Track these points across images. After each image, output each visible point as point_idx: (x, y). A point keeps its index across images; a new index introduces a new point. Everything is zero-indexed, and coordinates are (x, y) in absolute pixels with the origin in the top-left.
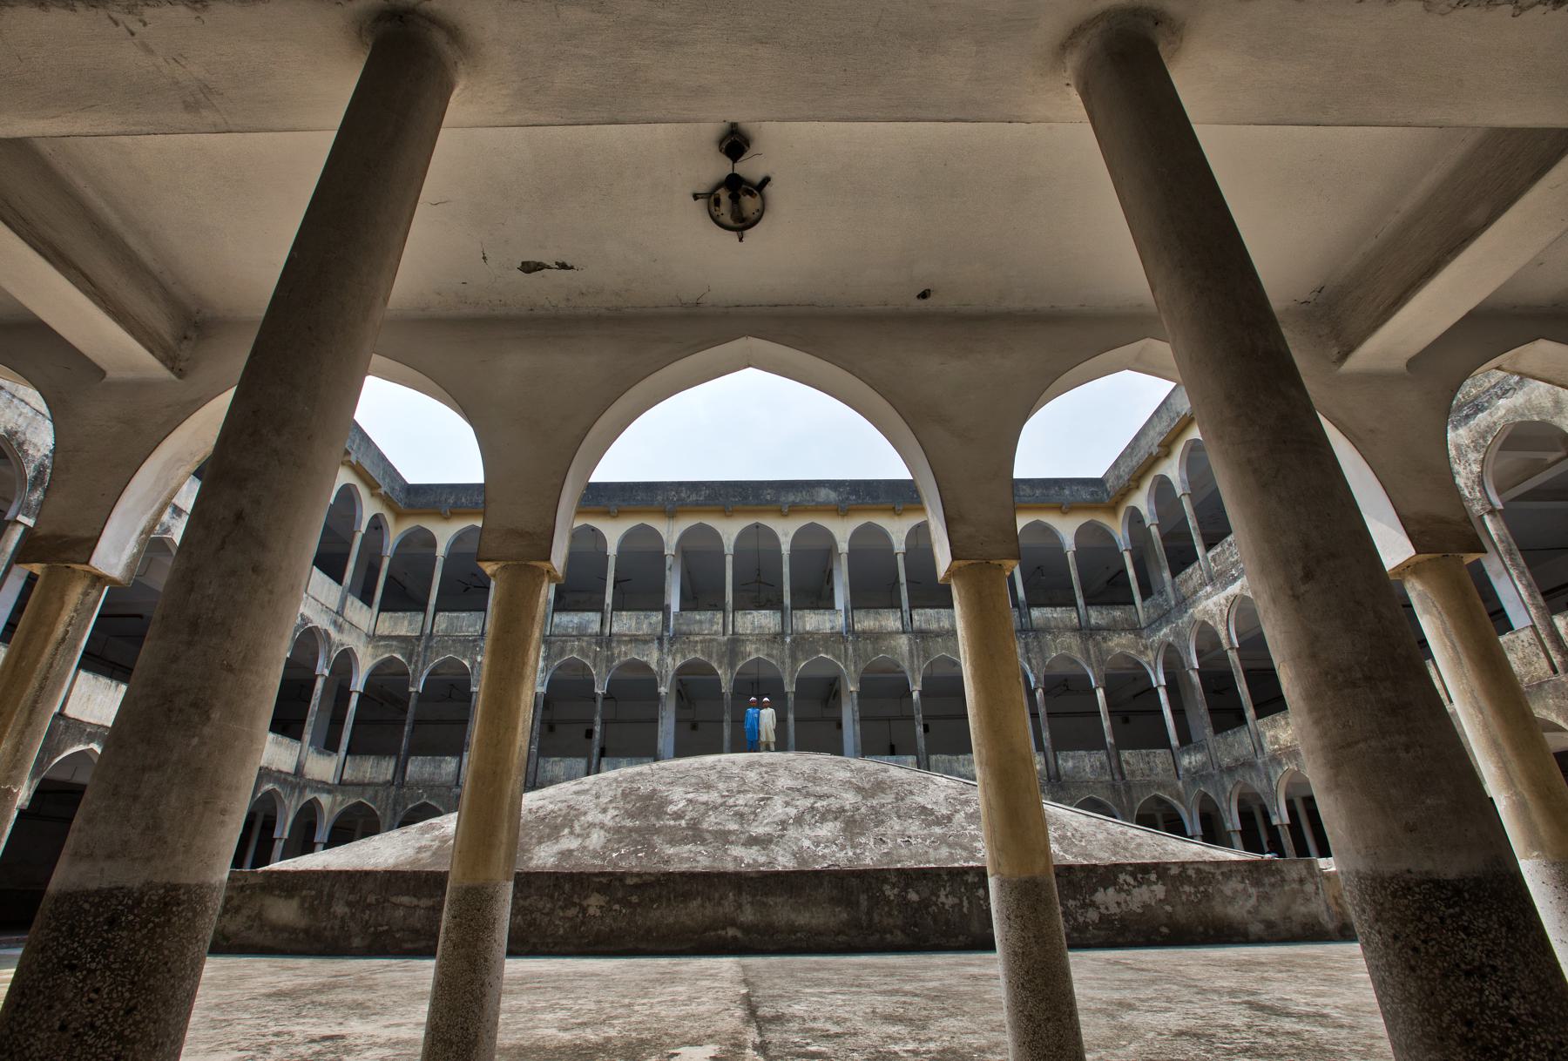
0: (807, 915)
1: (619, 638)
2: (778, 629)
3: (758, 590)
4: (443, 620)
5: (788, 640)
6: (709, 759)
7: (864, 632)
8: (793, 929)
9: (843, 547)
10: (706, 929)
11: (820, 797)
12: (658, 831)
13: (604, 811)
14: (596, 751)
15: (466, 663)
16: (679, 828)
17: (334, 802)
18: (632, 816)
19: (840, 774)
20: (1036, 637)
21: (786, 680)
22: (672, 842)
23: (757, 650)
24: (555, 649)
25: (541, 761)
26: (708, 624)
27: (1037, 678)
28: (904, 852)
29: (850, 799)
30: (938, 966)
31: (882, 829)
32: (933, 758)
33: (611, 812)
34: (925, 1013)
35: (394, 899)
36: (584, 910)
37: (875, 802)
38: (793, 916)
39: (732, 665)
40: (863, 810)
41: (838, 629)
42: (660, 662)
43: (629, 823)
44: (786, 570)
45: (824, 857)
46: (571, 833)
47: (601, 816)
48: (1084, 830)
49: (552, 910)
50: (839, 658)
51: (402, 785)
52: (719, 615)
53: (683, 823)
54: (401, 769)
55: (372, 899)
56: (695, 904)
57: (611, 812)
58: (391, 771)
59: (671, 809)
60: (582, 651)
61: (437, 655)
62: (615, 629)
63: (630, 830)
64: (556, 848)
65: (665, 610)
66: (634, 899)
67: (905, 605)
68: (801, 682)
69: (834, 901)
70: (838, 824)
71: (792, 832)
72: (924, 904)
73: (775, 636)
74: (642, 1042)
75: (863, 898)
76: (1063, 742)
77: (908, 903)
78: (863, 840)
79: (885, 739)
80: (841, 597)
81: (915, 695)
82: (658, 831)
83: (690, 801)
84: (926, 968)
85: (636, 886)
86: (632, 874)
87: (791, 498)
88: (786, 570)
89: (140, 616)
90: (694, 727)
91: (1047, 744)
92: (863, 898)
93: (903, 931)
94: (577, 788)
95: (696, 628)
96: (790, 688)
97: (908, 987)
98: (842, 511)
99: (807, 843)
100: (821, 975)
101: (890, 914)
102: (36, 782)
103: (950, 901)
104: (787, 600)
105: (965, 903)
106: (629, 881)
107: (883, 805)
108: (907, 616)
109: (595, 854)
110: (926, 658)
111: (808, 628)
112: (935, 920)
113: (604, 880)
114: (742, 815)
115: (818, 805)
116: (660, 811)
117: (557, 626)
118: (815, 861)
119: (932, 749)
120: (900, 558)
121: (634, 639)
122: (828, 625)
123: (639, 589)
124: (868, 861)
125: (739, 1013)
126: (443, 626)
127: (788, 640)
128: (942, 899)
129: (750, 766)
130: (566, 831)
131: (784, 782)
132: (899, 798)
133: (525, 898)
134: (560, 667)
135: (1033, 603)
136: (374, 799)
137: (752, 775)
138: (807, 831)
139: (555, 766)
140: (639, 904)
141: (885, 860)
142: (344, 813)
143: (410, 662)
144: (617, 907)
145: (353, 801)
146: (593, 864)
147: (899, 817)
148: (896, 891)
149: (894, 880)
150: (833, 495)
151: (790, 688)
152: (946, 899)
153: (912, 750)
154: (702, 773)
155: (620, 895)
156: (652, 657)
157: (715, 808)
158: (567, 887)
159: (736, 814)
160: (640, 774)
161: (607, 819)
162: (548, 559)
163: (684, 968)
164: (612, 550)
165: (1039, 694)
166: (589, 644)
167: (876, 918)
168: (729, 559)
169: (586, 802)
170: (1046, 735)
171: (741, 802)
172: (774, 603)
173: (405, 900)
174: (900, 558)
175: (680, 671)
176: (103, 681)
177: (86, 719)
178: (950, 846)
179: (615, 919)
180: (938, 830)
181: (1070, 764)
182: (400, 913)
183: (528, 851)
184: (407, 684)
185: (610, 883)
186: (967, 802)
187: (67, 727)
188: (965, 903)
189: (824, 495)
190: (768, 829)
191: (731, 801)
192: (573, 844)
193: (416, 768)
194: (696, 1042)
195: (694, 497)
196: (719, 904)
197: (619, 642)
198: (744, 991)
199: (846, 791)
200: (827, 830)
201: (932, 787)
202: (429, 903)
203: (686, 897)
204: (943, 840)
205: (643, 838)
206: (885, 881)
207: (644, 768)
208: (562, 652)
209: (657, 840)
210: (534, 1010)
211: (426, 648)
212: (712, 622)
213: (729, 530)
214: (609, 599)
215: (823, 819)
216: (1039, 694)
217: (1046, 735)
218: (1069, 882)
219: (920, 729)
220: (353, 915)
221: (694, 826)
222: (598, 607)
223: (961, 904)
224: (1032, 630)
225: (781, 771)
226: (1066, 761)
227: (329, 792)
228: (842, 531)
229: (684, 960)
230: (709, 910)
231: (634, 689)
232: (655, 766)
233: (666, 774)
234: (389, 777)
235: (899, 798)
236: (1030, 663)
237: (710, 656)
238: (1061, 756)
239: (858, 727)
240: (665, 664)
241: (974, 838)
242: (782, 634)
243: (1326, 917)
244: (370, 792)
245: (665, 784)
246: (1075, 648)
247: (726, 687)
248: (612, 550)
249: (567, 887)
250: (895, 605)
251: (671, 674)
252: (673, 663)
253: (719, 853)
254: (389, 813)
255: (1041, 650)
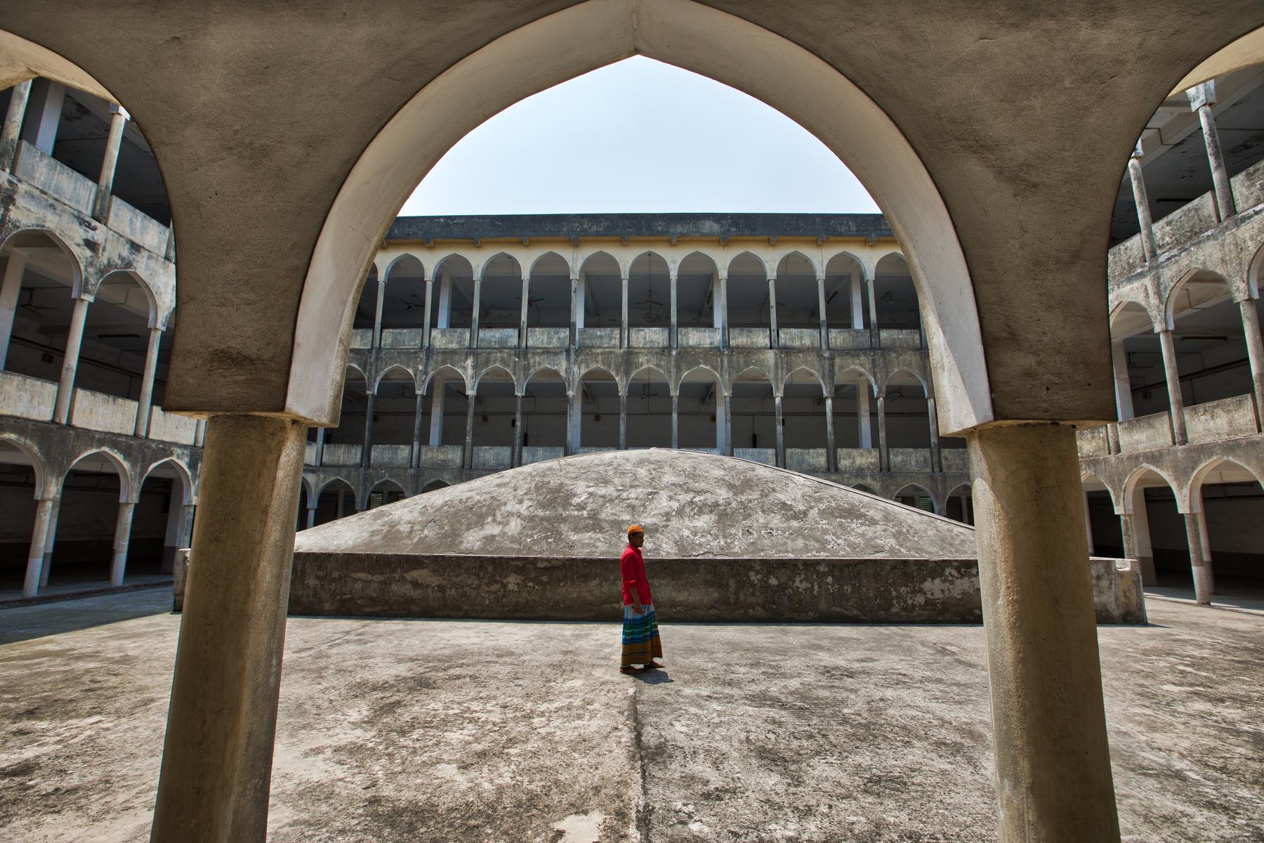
0: (686, 593)
1: (535, 350)
2: (666, 343)
3: (650, 308)
4: (389, 336)
5: (674, 353)
6: (609, 455)
7: (738, 347)
8: (674, 604)
9: (723, 274)
10: (603, 603)
11: (698, 493)
12: (564, 520)
13: (521, 502)
14: (518, 441)
15: (410, 371)
16: (581, 518)
17: (318, 479)
18: (543, 506)
19: (711, 467)
20: (883, 355)
21: (672, 386)
22: (576, 530)
23: (648, 361)
24: (482, 359)
25: (475, 449)
26: (608, 338)
27: (880, 388)
28: (767, 542)
29: (723, 494)
30: (794, 649)
31: (748, 522)
32: (789, 451)
33: (527, 503)
34: (795, 744)
35: (353, 575)
36: (505, 586)
37: (744, 498)
38: (674, 594)
39: (627, 374)
40: (734, 505)
41: (716, 344)
42: (568, 370)
43: (540, 513)
44: (673, 293)
45: (700, 545)
46: (494, 521)
47: (518, 506)
48: (917, 527)
49: (479, 586)
50: (716, 369)
51: (369, 467)
52: (617, 332)
53: (585, 513)
54: (366, 455)
55: (335, 574)
56: (594, 584)
57: (527, 503)
58: (359, 456)
59: (575, 501)
60: (503, 361)
61: (386, 365)
62: (530, 343)
63: (542, 519)
64: (482, 533)
65: (570, 325)
66: (545, 579)
67: (774, 326)
68: (685, 388)
69: (707, 583)
70: (713, 517)
71: (674, 523)
72: (782, 587)
73: (663, 349)
74: (533, 798)
75: (732, 582)
76: (895, 441)
77: (769, 587)
78: (733, 531)
79: (750, 438)
80: (720, 315)
81: (778, 400)
82: (564, 520)
83: (591, 494)
84: (783, 652)
85: (546, 569)
86: (542, 560)
87: (679, 229)
88: (673, 293)
89: (137, 336)
90: (597, 418)
91: (882, 442)
92: (732, 582)
93: (764, 608)
94: (499, 481)
95: (598, 342)
96: (675, 393)
97: (774, 688)
98: (723, 241)
99: (686, 533)
100: (698, 661)
101: (753, 594)
102: (62, 480)
103: (804, 585)
104: (674, 319)
105: (816, 587)
106: (540, 565)
107: (750, 501)
108: (774, 334)
109: (513, 539)
110: (789, 370)
111: (691, 343)
112: (790, 599)
113: (520, 564)
114: (633, 507)
115: (697, 499)
116: (566, 503)
117: (482, 340)
118: (693, 549)
119: (789, 444)
120: (772, 285)
121: (546, 352)
122: (708, 341)
123: (549, 306)
124: (737, 549)
125: (626, 736)
126: (389, 341)
127: (674, 353)
128: (797, 583)
129: (641, 463)
130: (490, 519)
131: (669, 478)
132: (764, 495)
133: (457, 576)
134: (487, 374)
135: (882, 325)
136: (348, 477)
137: (642, 472)
138: (687, 522)
139: (488, 454)
140: (548, 583)
141: (751, 549)
142: (329, 485)
143: (365, 370)
144: (531, 584)
145: (333, 478)
146: (510, 551)
147: (763, 512)
148: (759, 576)
149: (758, 568)
150: (716, 227)
151: (675, 393)
152: (800, 584)
153: (772, 444)
154: (601, 469)
155: (533, 575)
156: (561, 366)
157: (611, 501)
158: (490, 568)
159: (628, 506)
160: (550, 469)
161: (523, 509)
162: (282, 407)
163: (583, 643)
164: (526, 275)
165: (880, 402)
166: (510, 355)
167: (742, 597)
168: (625, 284)
169: (506, 493)
170: (882, 435)
171: (632, 496)
172: (660, 320)
173: (362, 575)
174: (772, 285)
175: (585, 377)
176: (101, 397)
177: (93, 428)
178: (805, 538)
179: (530, 594)
180: (795, 524)
181: (900, 458)
182: (359, 585)
183: (459, 536)
184: (364, 388)
185: (525, 566)
186: (821, 499)
187: (78, 436)
188: (816, 587)
189: (708, 226)
190: (654, 520)
191: (624, 495)
192: (494, 530)
193: (379, 453)
194: (580, 809)
195: (594, 228)
196: (614, 583)
197: (534, 354)
198: (631, 691)
199: (720, 487)
200: (703, 522)
201: (792, 485)
202: (381, 578)
203: (587, 578)
204: (799, 533)
205: (551, 526)
206: (751, 568)
207: (553, 464)
208: (487, 362)
209: (564, 528)
210: (445, 723)
211: (377, 359)
212: (611, 338)
213: (625, 258)
214: (524, 318)
215: (701, 512)
216: (880, 402)
217: (882, 435)
218: (904, 573)
219: (779, 428)
220: (322, 587)
221: (594, 516)
222: (515, 324)
223: (812, 589)
224: (880, 348)
225: (667, 468)
226: (896, 456)
227: (313, 472)
228: (723, 259)
229: (586, 628)
230: (605, 589)
231: (548, 393)
232: (564, 461)
233: (571, 469)
234: (358, 460)
235: (764, 495)
236: (875, 376)
237: (609, 366)
238: (892, 452)
239: (729, 425)
240: (572, 372)
241: (825, 532)
242: (669, 348)
243: (1114, 606)
244: (344, 472)
245: (572, 478)
246: (914, 365)
247: (622, 391)
248: (526, 275)
249: (490, 568)
250: (767, 325)
251: (577, 380)
252: (579, 371)
253: (614, 540)
254: (361, 488)
255: (886, 365)
